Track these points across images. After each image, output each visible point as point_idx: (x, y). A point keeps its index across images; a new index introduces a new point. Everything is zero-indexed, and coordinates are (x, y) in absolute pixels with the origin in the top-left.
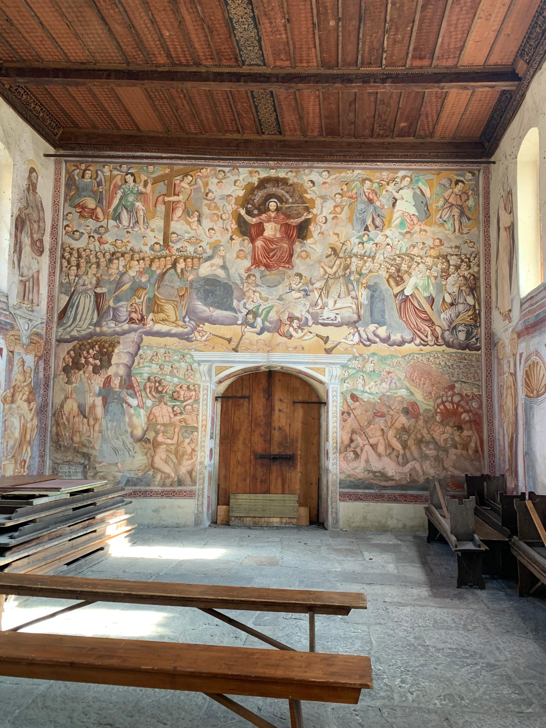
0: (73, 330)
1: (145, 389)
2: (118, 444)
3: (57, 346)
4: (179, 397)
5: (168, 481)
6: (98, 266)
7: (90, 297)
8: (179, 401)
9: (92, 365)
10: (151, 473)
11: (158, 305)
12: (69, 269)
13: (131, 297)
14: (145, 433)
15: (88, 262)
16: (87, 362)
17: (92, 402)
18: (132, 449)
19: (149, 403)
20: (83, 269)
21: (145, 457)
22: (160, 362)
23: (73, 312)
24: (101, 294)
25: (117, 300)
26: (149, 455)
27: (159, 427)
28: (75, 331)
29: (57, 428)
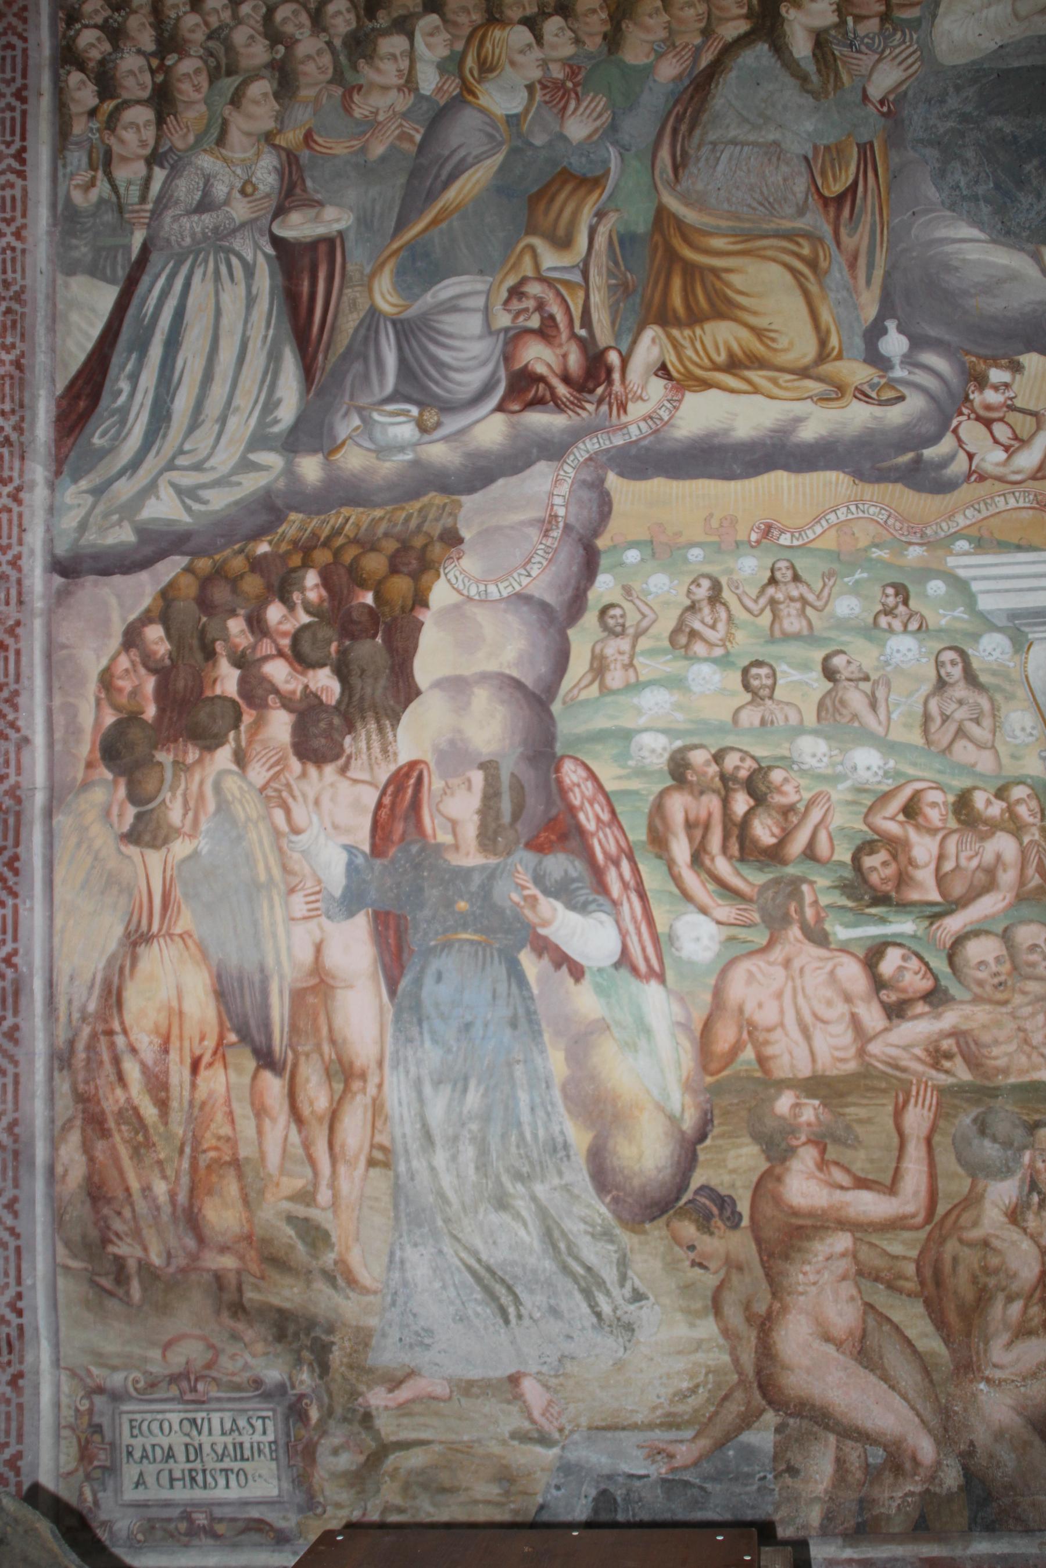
0: (151, 489)
1: (659, 841)
2: (511, 1240)
3: (60, 598)
4: (903, 879)
5: (895, 1498)
6: (285, 79)
7: (249, 271)
8: (904, 906)
9: (287, 702)
10: (762, 1437)
11: (690, 271)
12: (112, 123)
13: (509, 245)
14: (689, 1151)
15: (223, 65)
16: (256, 691)
17: (305, 955)
18: (609, 1274)
19: (698, 937)
20: (194, 112)
21: (708, 1328)
22: (746, 644)
23: (148, 378)
24: (314, 245)
25: (422, 268)
26: (734, 1316)
27: (784, 1103)
28: (166, 492)
29: (87, 1148)
